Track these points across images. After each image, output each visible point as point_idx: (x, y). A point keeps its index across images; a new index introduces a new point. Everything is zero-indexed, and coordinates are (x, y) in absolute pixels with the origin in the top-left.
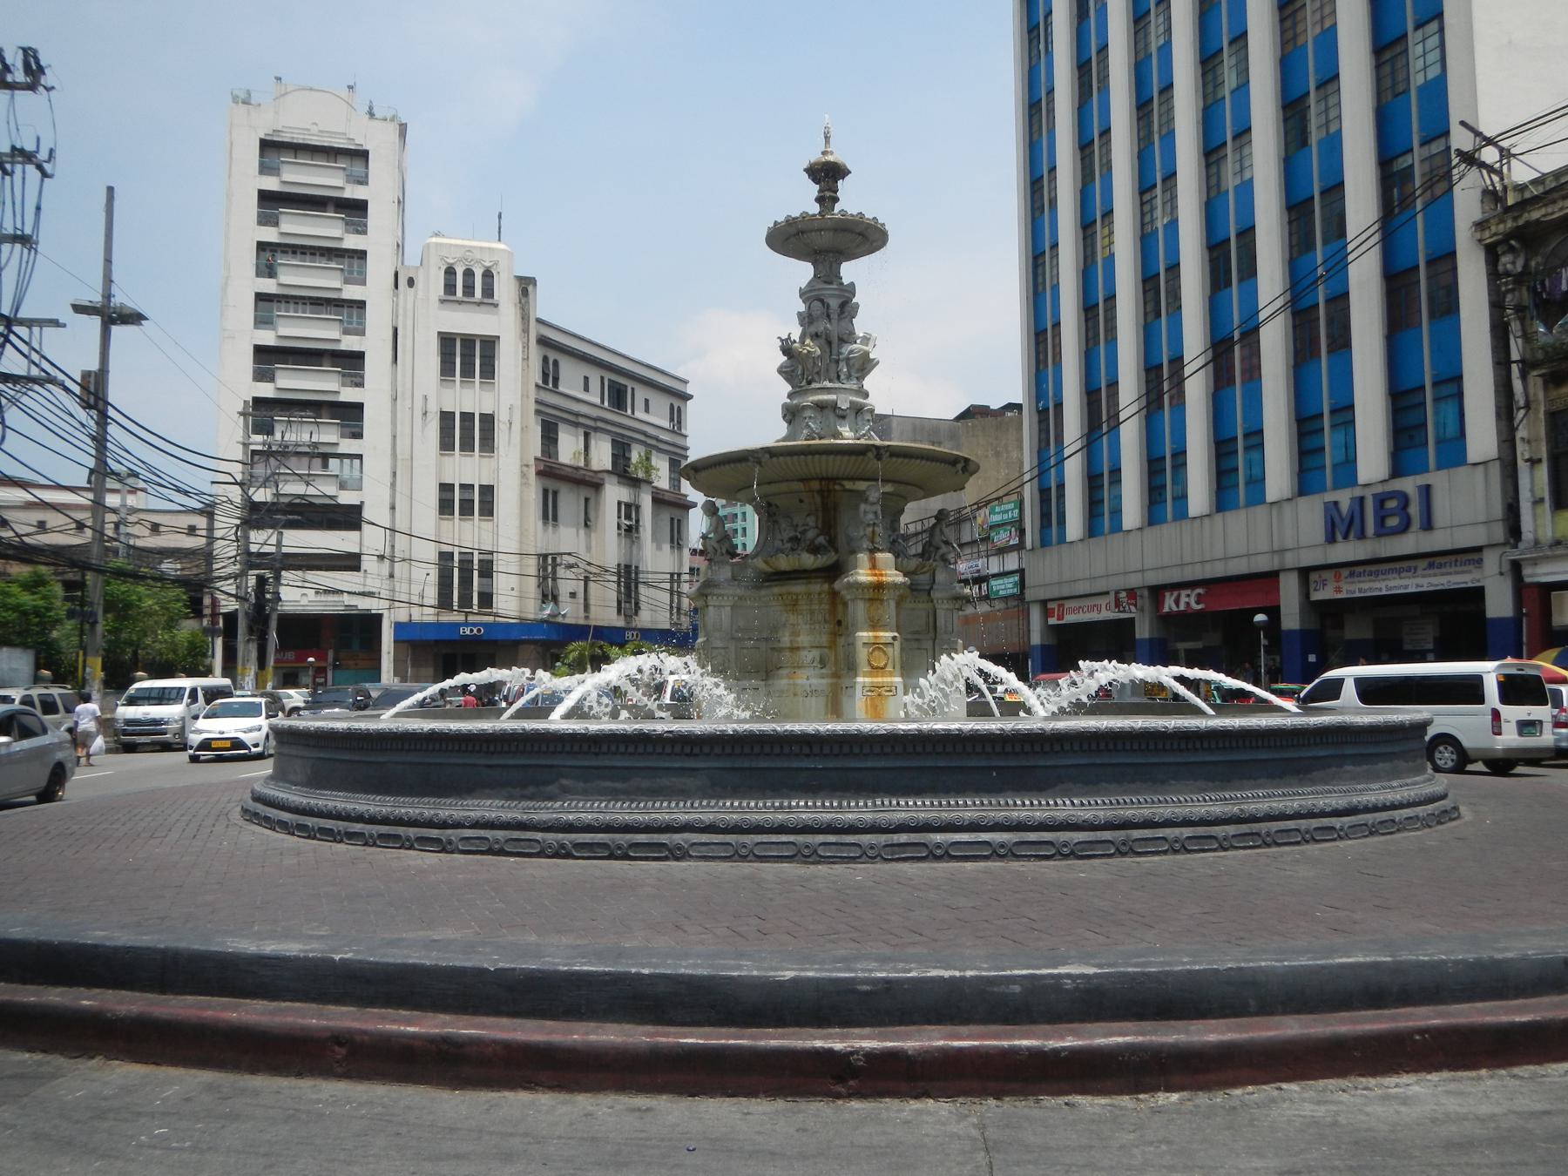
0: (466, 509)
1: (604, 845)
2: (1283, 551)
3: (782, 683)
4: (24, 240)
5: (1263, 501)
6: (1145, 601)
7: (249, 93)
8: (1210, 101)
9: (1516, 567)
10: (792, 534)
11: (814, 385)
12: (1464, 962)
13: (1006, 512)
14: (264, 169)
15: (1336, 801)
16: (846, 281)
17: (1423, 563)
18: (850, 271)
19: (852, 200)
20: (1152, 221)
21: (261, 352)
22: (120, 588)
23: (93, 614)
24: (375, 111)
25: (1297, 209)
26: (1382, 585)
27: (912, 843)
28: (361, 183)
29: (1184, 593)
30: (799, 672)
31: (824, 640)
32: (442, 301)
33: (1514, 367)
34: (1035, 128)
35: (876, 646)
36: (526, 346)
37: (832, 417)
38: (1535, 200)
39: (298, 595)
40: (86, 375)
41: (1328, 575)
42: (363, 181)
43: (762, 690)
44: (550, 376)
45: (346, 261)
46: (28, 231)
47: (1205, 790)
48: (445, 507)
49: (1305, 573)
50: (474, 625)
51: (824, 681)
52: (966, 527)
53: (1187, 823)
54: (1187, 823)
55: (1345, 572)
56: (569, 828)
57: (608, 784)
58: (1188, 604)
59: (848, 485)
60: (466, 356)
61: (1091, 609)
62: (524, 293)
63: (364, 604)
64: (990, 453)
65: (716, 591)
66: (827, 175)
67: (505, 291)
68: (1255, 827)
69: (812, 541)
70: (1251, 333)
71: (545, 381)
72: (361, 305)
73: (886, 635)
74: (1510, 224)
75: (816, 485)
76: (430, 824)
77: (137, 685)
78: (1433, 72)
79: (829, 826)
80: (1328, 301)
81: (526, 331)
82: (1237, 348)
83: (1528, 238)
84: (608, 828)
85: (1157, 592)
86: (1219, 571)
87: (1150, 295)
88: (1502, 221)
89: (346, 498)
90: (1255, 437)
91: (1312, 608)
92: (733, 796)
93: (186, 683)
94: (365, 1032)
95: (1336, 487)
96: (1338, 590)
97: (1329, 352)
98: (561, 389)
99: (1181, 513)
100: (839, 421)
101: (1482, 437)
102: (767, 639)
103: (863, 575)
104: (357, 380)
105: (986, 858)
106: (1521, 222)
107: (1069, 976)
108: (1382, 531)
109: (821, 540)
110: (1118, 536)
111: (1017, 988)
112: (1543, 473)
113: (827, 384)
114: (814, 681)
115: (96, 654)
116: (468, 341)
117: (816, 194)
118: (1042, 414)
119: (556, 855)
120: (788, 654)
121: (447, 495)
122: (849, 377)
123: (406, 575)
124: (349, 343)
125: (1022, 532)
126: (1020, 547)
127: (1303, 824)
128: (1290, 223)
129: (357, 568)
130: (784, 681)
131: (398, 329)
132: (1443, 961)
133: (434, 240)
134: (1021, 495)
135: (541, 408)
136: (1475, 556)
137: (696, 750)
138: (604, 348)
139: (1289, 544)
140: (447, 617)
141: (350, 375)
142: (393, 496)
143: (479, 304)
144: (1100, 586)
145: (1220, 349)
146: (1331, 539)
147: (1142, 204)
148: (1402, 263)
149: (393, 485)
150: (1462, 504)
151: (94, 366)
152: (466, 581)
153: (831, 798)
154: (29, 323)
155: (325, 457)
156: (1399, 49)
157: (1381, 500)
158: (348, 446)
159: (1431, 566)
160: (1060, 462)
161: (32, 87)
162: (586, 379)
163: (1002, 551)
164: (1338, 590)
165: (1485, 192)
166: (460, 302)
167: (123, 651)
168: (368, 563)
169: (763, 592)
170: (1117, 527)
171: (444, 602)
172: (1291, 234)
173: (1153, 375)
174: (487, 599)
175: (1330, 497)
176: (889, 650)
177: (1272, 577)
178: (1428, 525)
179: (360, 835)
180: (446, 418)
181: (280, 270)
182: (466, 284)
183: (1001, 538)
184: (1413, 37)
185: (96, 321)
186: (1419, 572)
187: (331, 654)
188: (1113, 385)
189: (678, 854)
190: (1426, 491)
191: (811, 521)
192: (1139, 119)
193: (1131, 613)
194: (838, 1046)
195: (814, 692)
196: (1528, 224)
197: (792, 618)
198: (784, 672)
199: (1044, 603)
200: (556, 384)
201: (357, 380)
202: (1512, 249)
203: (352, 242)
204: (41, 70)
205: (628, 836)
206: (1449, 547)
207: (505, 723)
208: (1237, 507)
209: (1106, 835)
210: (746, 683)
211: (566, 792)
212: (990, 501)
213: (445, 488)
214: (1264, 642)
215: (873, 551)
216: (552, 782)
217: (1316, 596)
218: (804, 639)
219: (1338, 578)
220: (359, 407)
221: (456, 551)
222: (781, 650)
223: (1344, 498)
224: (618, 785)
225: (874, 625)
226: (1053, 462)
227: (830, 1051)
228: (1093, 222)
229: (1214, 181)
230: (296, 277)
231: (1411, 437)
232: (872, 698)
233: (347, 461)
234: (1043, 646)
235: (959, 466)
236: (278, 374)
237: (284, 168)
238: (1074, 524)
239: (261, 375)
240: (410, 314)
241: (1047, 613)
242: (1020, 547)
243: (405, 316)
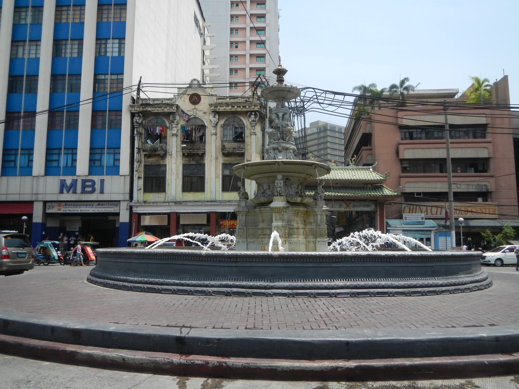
2: (37, 194)
5: (30, 174)
8: (16, 22)
9: (131, 208)
17: (97, 203)
25: (56, 78)
26: (79, 209)
31: (304, 226)
33: (136, 150)
38: (149, 105)
41: (56, 204)
49: (45, 203)
55: (63, 204)
70: (32, 114)
74: (141, 109)
78: (116, 54)
79: (294, 287)
83: (145, 114)
88: (139, 108)
91: (46, 216)
95: (63, 175)
96: (60, 210)
97: (66, 129)
101: (124, 167)
106: (145, 110)
108: (83, 192)
112: (141, 182)
120: (296, 230)
130: (296, 239)
136: (116, 203)
139: (41, 192)
146: (61, 192)
148: (100, 107)
150: (115, 187)
156: (103, 42)
157: (84, 182)
159: (99, 205)
165: (133, 98)
175: (62, 178)
177: (31, 203)
178: (102, 192)
179: (448, 291)
184: (110, 41)
186: (94, 206)
190: (102, 181)
196: (146, 111)
197: (296, 218)
202: (139, 116)
206: (109, 200)
208: (15, 175)
217: (48, 211)
222: (293, 228)
223: (69, 180)
231: (94, 163)
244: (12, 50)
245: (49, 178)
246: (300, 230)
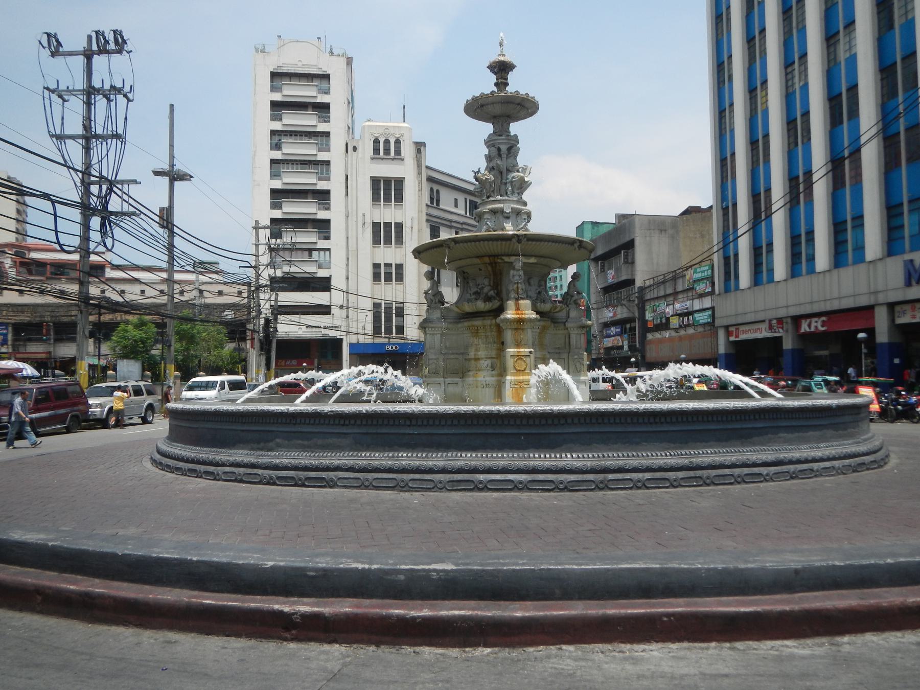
0: (388, 278)
1: (292, 478)
2: (876, 293)
3: (470, 380)
4: (117, 136)
6: (789, 326)
7: (264, 46)
10: (476, 289)
11: (491, 199)
12: (715, 569)
13: (703, 272)
14: (274, 89)
15: (768, 456)
16: (512, 134)
18: (515, 128)
19: (516, 84)
20: (793, 84)
21: (275, 193)
22: (186, 327)
23: (169, 341)
24: (335, 52)
27: (464, 481)
28: (326, 93)
29: (814, 320)
30: (480, 373)
31: (494, 353)
32: (372, 159)
34: (719, 31)
35: (519, 357)
36: (420, 183)
37: (501, 218)
39: (289, 328)
40: (162, 210)
41: (907, 307)
42: (327, 92)
43: (460, 384)
44: (434, 200)
45: (319, 138)
46: (120, 131)
47: (668, 449)
48: (376, 277)
49: (891, 306)
50: (394, 344)
51: (493, 379)
52: (680, 282)
53: (648, 469)
54: (648, 469)
56: (276, 467)
57: (300, 442)
58: (816, 327)
59: (506, 259)
60: (387, 190)
61: (756, 331)
62: (419, 151)
63: (332, 333)
64: (698, 235)
65: (430, 325)
66: (502, 69)
67: (408, 151)
68: (699, 473)
69: (487, 294)
70: (856, 152)
71: (432, 202)
72: (328, 163)
73: (525, 350)
75: (487, 260)
76: (211, 463)
77: (193, 380)
80: (907, 130)
81: (420, 173)
82: (847, 162)
84: (296, 468)
85: (797, 320)
86: (835, 305)
87: (792, 132)
89: (322, 273)
90: (859, 220)
92: (367, 450)
93: (218, 378)
94: (50, 588)
95: (912, 250)
96: (914, 317)
98: (441, 207)
99: (811, 270)
100: (505, 220)
102: (462, 354)
103: (510, 314)
104: (327, 206)
105: (510, 490)
107: (435, 570)
109: (492, 293)
110: (772, 285)
111: (402, 577)
113: (499, 198)
114: (488, 379)
115: (171, 363)
116: (387, 181)
117: (495, 81)
118: (725, 210)
119: (268, 483)
120: (473, 362)
121: (378, 270)
122: (513, 193)
123: (355, 317)
124: (322, 185)
125: (713, 284)
126: (712, 293)
127: (737, 471)
128: (882, 80)
129: (328, 313)
131: (349, 177)
132: (698, 569)
133: (367, 123)
134: (712, 260)
135: (430, 218)
137: (347, 422)
138: (466, 181)
139: (880, 288)
140: (377, 340)
141: (323, 204)
142: (347, 271)
143: (393, 159)
144: (760, 317)
145: (836, 163)
146: (908, 284)
147: (787, 74)
149: (347, 265)
151: (166, 204)
152: (389, 320)
153: (423, 451)
154: (122, 182)
155: (310, 251)
158: (322, 244)
160: (736, 239)
161: (119, 52)
162: (456, 200)
163: (701, 296)
164: (914, 317)
166: (382, 159)
167: (192, 361)
168: (334, 310)
169: (460, 325)
170: (771, 279)
171: (377, 331)
172: (882, 87)
173: (794, 183)
174: (400, 330)
175: (907, 257)
176: (528, 360)
177: (870, 308)
180: (376, 226)
181: (283, 146)
182: (386, 148)
183: (701, 287)
185: (166, 180)
187: (316, 361)
188: (768, 190)
189: (331, 484)
191: (486, 282)
192: (784, 20)
193: (780, 333)
194: (286, 609)
195: (488, 385)
197: (476, 341)
198: (471, 373)
199: (727, 328)
200: (438, 204)
201: (327, 206)
203: (322, 127)
204: (124, 42)
205: (306, 473)
207: (299, 405)
208: (847, 265)
209: (591, 477)
210: (449, 380)
211: (279, 447)
212: (691, 267)
213: (376, 266)
214: (864, 351)
215: (517, 299)
216: (272, 441)
217: (899, 321)
218: (482, 354)
219: (913, 309)
220: (327, 222)
221: (383, 303)
222: (469, 360)
224: (306, 443)
225: (518, 345)
226: (731, 238)
227: (282, 612)
228: (755, 88)
229: (832, 57)
230: (292, 149)
232: (516, 389)
233: (322, 253)
234: (727, 355)
235: (576, 245)
236: (284, 204)
237: (284, 87)
238: (745, 278)
239: (275, 206)
240: (354, 166)
241: (728, 334)
242: (712, 293)
243: (352, 168)
244: (829, 54)
245: (889, 260)
246: (482, 362)
